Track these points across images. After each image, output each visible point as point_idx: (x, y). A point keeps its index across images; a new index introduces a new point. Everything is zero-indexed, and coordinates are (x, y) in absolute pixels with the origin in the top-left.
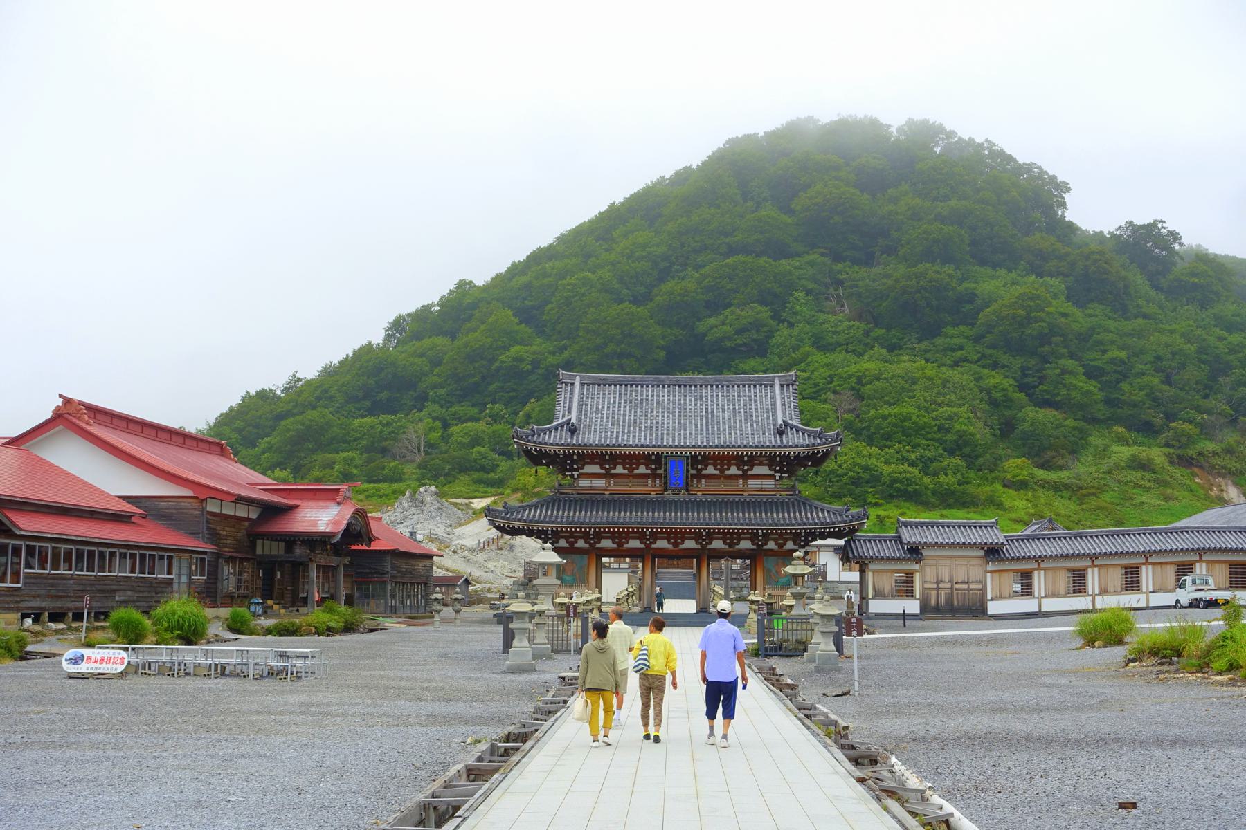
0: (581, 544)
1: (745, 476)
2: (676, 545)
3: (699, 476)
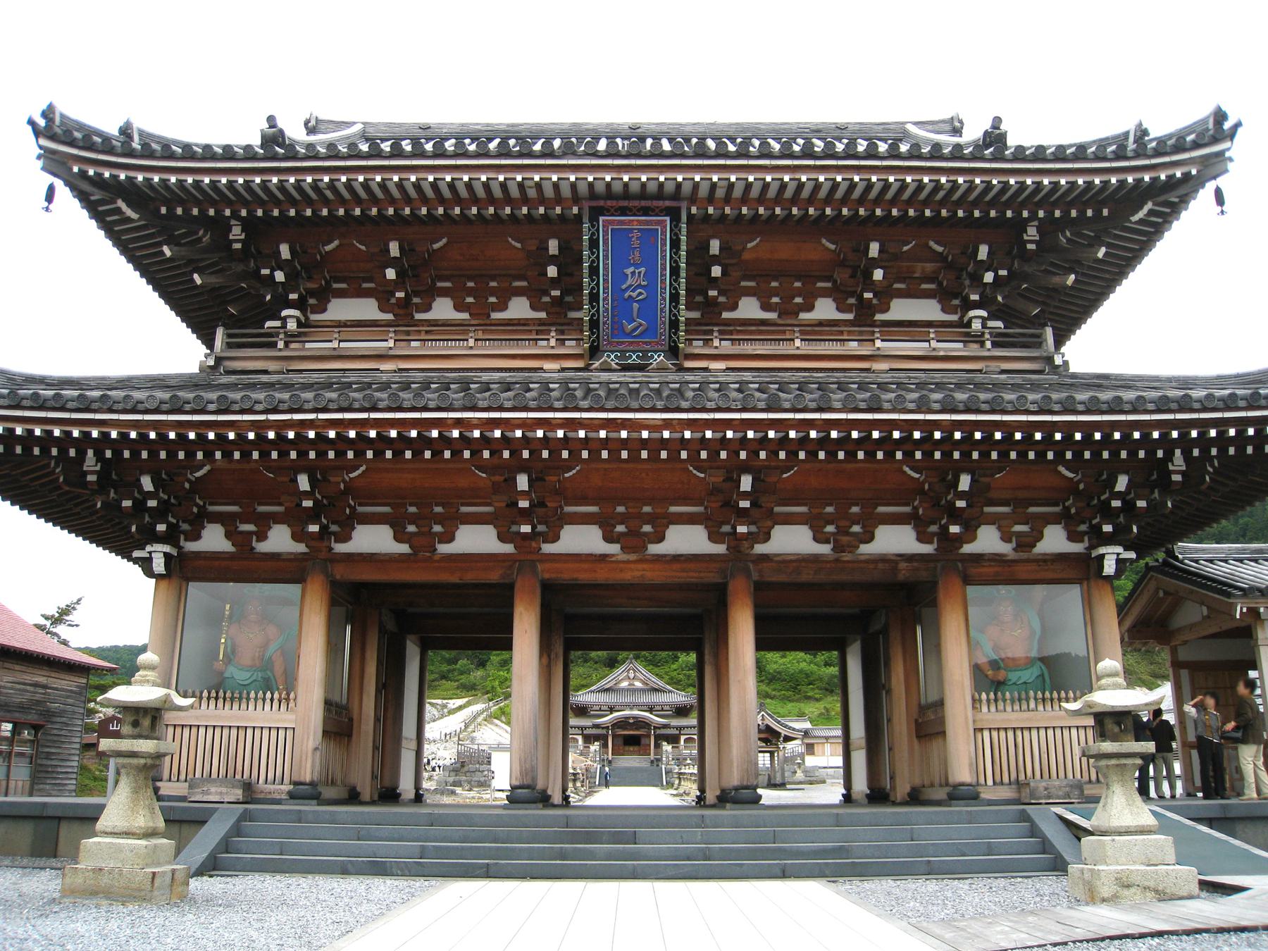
0: (280, 540)
1: (866, 320)
2: (634, 542)
3: (710, 318)
